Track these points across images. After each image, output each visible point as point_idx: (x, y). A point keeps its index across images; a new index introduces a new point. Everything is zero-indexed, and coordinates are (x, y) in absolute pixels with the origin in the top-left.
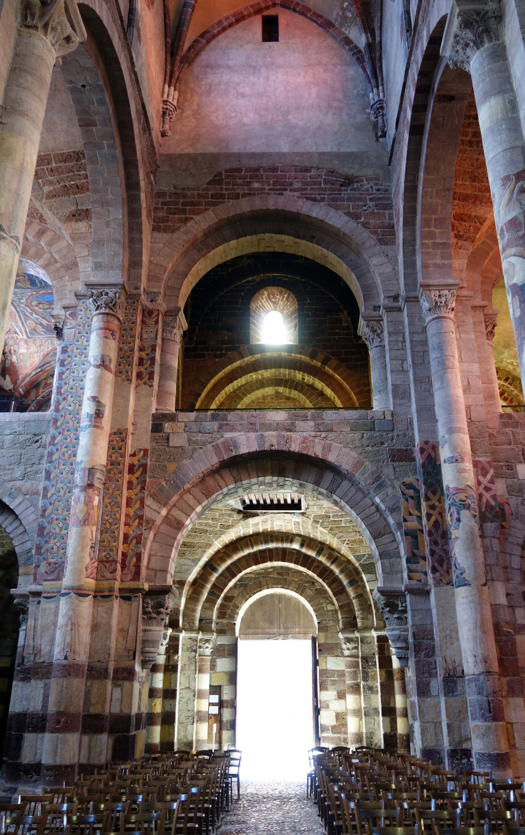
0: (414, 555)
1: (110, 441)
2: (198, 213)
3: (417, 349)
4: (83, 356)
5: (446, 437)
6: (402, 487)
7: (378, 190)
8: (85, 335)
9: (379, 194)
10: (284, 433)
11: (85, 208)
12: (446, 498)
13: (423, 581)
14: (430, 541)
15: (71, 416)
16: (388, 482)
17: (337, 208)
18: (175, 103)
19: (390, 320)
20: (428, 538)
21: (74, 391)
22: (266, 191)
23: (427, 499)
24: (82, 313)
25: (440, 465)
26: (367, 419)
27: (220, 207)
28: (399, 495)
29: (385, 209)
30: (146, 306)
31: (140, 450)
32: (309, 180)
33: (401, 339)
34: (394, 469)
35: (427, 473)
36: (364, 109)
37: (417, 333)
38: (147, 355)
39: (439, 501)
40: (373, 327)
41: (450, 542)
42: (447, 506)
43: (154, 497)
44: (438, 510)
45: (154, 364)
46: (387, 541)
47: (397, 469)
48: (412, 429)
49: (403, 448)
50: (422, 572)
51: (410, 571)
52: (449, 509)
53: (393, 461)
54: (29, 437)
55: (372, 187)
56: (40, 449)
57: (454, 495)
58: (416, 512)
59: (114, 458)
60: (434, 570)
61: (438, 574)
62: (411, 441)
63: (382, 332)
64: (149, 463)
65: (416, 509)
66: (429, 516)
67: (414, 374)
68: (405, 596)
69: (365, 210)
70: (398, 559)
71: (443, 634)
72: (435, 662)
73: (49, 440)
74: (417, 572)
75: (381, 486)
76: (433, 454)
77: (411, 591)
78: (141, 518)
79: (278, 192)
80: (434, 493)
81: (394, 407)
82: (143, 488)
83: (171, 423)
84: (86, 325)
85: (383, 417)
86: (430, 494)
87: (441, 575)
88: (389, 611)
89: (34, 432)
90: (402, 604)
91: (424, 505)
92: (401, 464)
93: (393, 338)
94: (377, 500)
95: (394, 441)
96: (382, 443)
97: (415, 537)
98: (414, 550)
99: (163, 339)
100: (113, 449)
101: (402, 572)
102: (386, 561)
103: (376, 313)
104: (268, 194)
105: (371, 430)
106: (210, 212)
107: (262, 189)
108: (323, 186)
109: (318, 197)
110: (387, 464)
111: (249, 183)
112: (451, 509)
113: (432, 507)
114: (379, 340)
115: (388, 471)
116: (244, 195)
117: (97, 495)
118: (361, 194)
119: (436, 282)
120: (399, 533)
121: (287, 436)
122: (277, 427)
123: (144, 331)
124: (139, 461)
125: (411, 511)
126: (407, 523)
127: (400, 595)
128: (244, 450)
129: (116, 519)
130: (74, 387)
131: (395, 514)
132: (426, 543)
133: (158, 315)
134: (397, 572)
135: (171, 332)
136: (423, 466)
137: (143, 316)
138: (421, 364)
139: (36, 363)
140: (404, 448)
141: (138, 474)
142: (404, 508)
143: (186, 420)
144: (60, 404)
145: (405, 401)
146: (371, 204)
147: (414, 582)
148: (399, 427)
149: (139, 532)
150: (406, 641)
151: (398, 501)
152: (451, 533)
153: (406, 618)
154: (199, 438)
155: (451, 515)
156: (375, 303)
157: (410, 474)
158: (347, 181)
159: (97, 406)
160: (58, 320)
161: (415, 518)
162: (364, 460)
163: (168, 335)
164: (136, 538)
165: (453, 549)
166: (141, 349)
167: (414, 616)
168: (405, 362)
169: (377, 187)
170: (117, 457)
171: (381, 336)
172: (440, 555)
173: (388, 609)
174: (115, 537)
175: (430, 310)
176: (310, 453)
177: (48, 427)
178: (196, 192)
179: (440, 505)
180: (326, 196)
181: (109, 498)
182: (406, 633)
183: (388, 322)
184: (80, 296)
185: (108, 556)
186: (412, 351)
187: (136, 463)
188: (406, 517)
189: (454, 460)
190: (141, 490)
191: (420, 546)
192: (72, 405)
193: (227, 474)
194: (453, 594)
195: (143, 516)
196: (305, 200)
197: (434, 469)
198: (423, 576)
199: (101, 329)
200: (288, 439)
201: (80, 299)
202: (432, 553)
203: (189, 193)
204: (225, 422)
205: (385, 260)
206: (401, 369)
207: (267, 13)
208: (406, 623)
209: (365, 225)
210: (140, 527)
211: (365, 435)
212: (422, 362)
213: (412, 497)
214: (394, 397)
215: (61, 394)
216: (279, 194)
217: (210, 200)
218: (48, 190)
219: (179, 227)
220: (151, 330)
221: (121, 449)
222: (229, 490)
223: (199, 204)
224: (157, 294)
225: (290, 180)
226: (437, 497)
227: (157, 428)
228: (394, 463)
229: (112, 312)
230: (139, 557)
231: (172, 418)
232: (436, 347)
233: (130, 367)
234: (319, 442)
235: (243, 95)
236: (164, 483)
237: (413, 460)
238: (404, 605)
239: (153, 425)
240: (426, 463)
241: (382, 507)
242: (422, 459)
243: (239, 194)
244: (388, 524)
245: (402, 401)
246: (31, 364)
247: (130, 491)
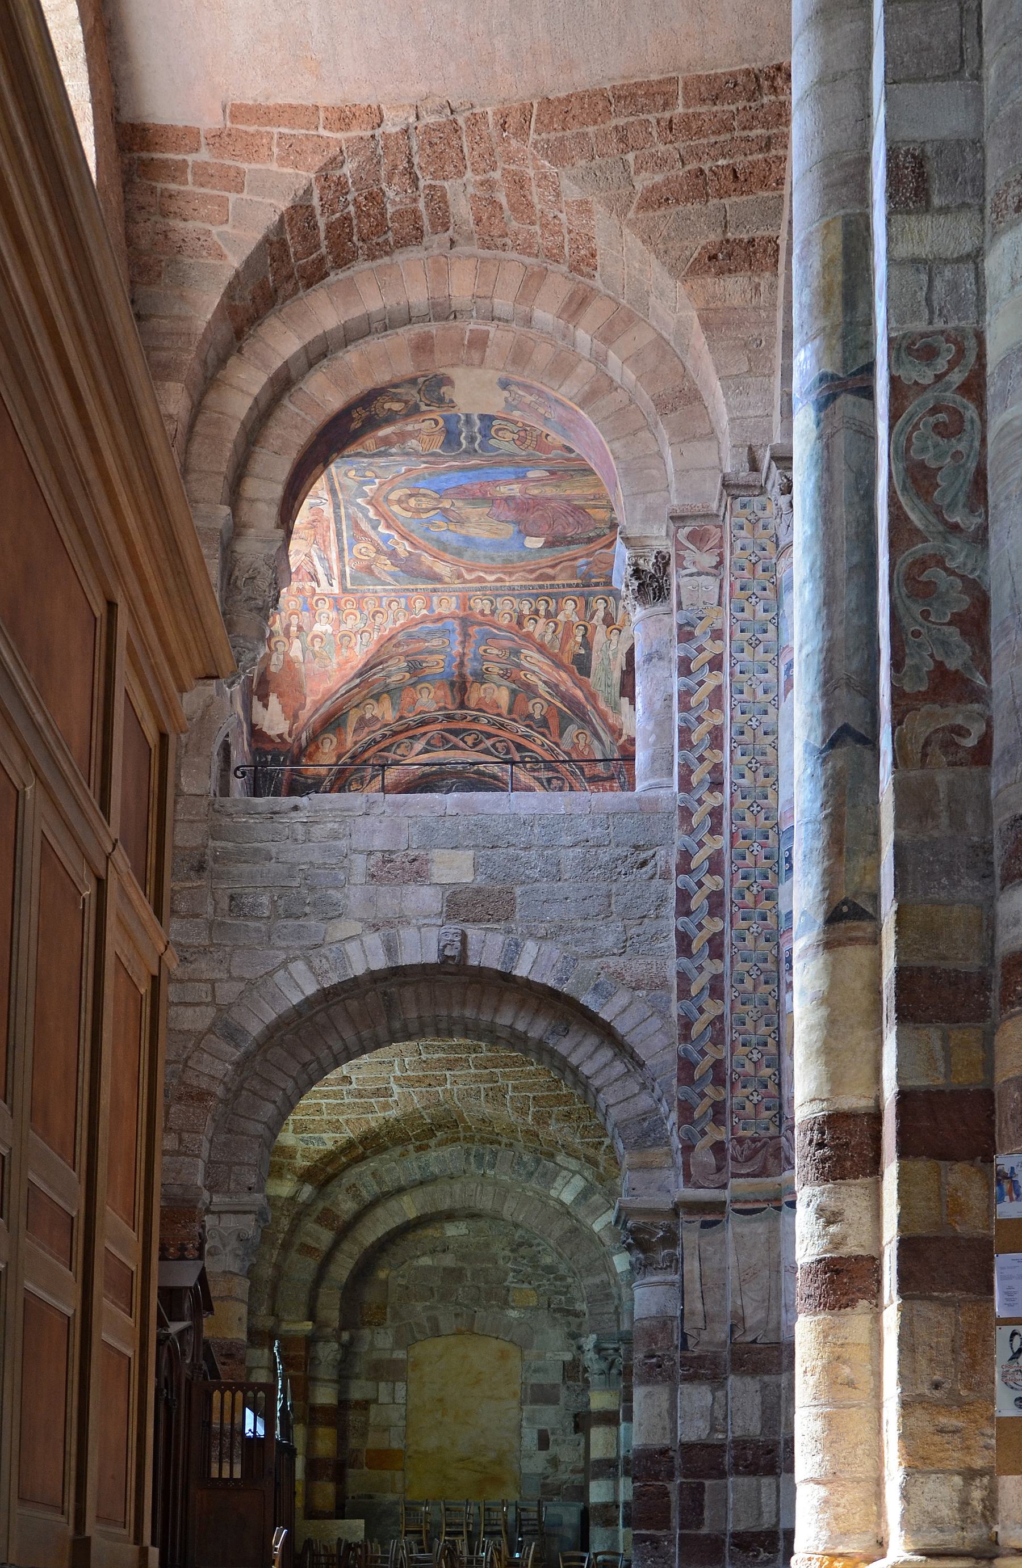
8: (759, 593)
15: (748, 802)
21: (747, 738)
54: (623, 851)
56: (657, 882)
73: (674, 860)
89: (633, 841)
130: (747, 729)
139: (354, 663)
144: (692, 772)
177: (669, 829)
184: (737, 486)
192: (748, 773)
215: (693, 747)
246: (341, 666)
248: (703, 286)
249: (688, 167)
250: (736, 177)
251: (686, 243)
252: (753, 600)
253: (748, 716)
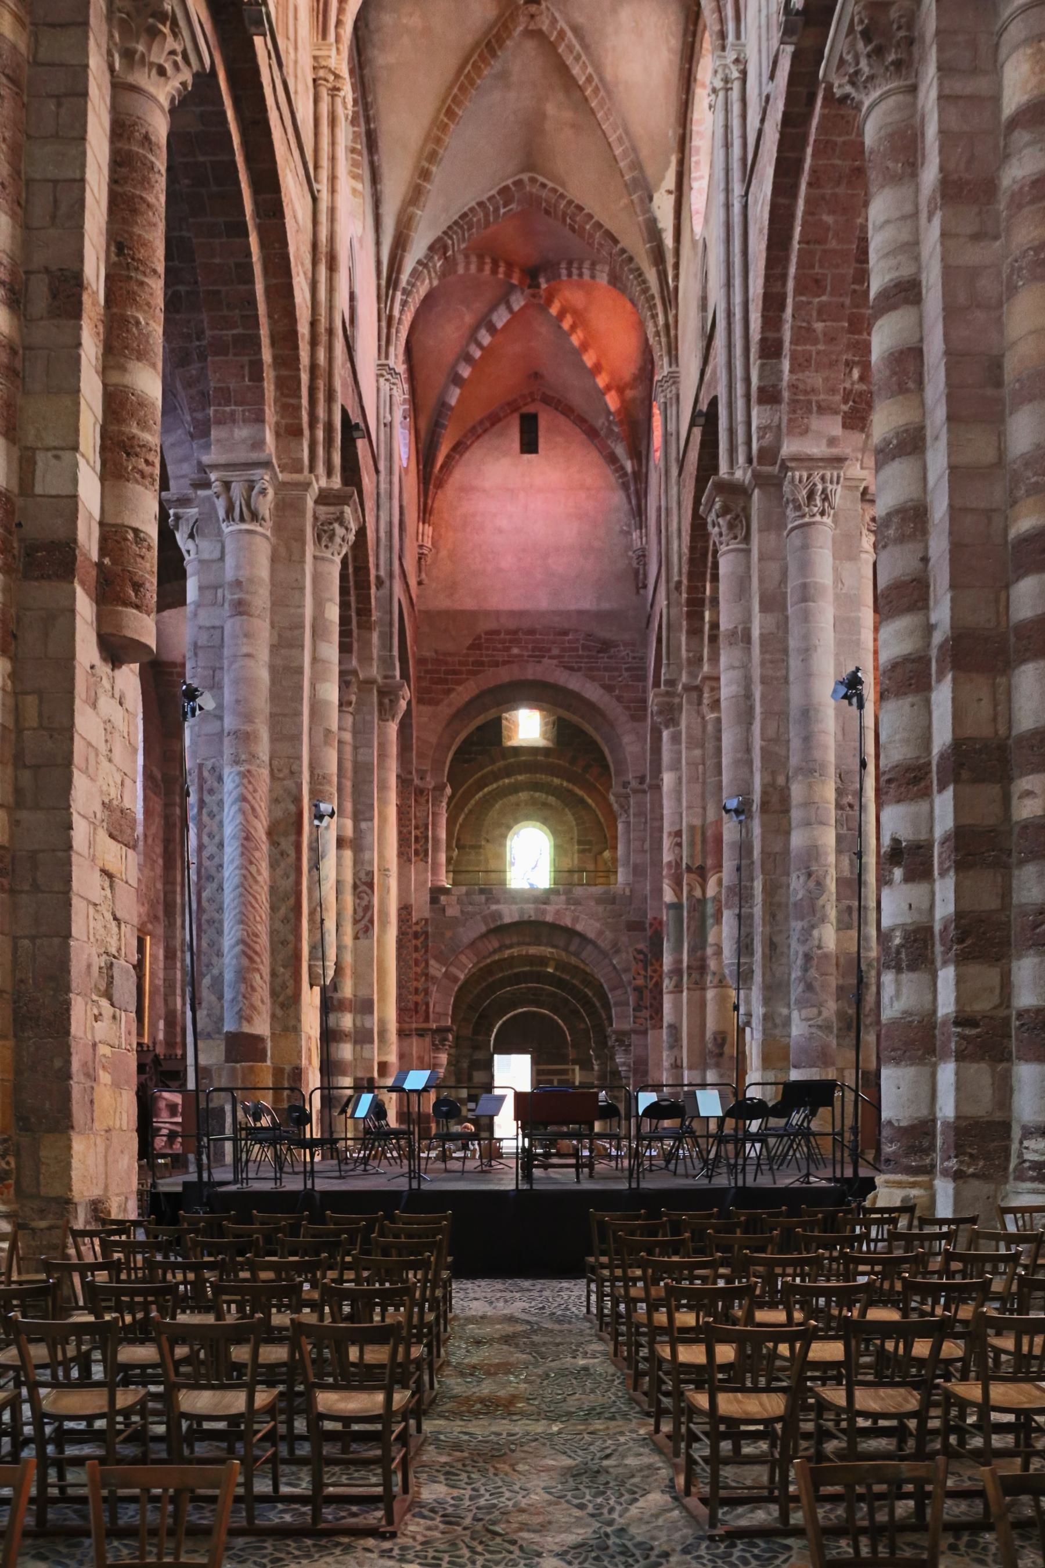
2: (459, 683)
17: (593, 679)
18: (429, 545)
36: (626, 552)
43: (436, 958)
51: (635, 1017)
78: (427, 975)
82: (426, 951)
111: (508, 649)
113: (655, 971)
115: (624, 939)
116: (505, 663)
128: (507, 920)
141: (422, 939)
146: (626, 674)
163: (437, 810)
166: (416, 828)
178: (456, 659)
202: (651, 1005)
203: (449, 659)
207: (525, 410)
209: (619, 699)
223: (460, 672)
224: (426, 771)
227: (434, 900)
230: (427, 1005)
235: (500, 531)
237: (645, 930)
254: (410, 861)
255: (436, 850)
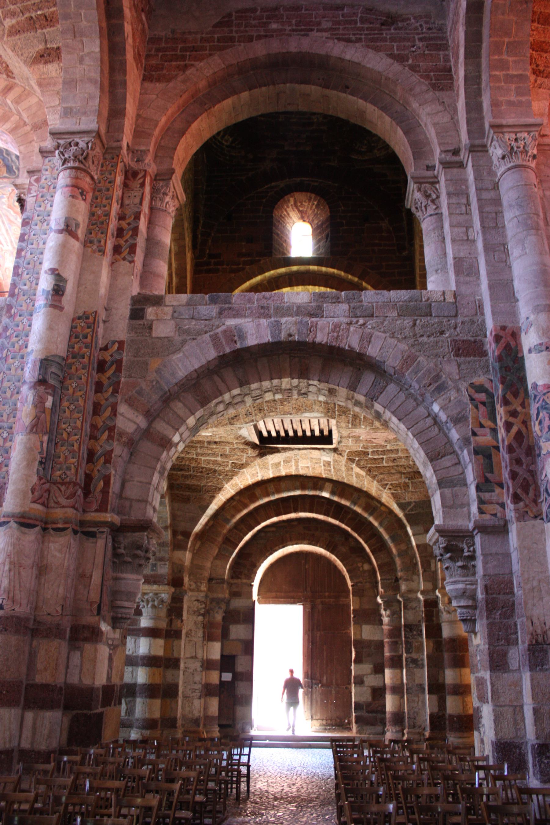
0: (487, 480)
1: (73, 328)
2: (200, 59)
3: (487, 209)
4: (45, 223)
5: (532, 317)
6: (470, 390)
7: (429, 29)
8: (49, 198)
9: (432, 33)
10: (306, 319)
11: (55, 46)
12: (532, 401)
13: (499, 515)
14: (511, 459)
15: (25, 298)
16: (450, 383)
17: (377, 49)
19: (449, 178)
20: (507, 456)
21: (30, 266)
22: (287, 32)
23: (506, 402)
24: (47, 173)
25: (523, 357)
26: (421, 301)
27: (228, 51)
28: (465, 401)
29: (439, 50)
30: (129, 166)
31: (114, 342)
32: (341, 18)
33: (464, 201)
34: (459, 366)
35: (506, 368)
37: (487, 189)
38: (129, 224)
39: (523, 405)
40: (425, 192)
41: (539, 460)
42: (533, 412)
44: (520, 417)
45: (137, 235)
46: (449, 464)
47: (463, 366)
48: (482, 314)
49: (470, 338)
50: (498, 504)
51: (481, 502)
52: (538, 414)
53: (457, 355)
55: (421, 26)
57: (544, 394)
58: (490, 423)
59: (76, 349)
60: (516, 498)
61: (521, 504)
62: (481, 330)
63: (438, 197)
64: (125, 358)
65: (490, 419)
66: (508, 426)
67: (485, 240)
68: (472, 537)
69: (413, 52)
70: (464, 489)
71: (529, 586)
72: (516, 625)
74: (492, 503)
75: (441, 389)
76: (512, 343)
77: (482, 528)
78: (111, 429)
79: (303, 33)
80: (516, 395)
81: (457, 286)
83: (155, 308)
84: (52, 187)
85: (442, 298)
86: (509, 396)
87: (526, 506)
88: (451, 558)
90: (469, 547)
91: (501, 411)
92: (468, 359)
93: (454, 200)
94: (436, 408)
95: (458, 329)
96: (442, 333)
97: (489, 457)
98: (487, 474)
99: (151, 209)
100: (77, 337)
101: (469, 505)
102: (447, 491)
103: (429, 173)
104: (290, 35)
105: (427, 315)
106: (216, 57)
107: (281, 30)
108: (359, 25)
109: (354, 38)
110: (449, 361)
112: (541, 415)
113: (514, 414)
114: (434, 207)
116: (259, 37)
117: (50, 395)
118: (407, 34)
119: (511, 121)
120: (465, 452)
121: (312, 322)
122: (300, 310)
123: (125, 195)
124: (112, 356)
125: (483, 421)
126: (477, 438)
127: (467, 536)
128: (251, 341)
129: (76, 428)
130: (32, 262)
131: (461, 425)
132: (503, 464)
133: (144, 176)
134: (462, 506)
135: (162, 200)
136: (500, 359)
137: (126, 178)
138: (493, 228)
140: (472, 339)
142: (473, 418)
143: (175, 303)
145: (471, 279)
147: (487, 517)
148: (465, 312)
149: (108, 448)
150: (473, 597)
151: (465, 409)
152: (540, 448)
153: (474, 566)
154: (191, 326)
155: (540, 423)
156: (427, 162)
157: (480, 373)
158: (390, 20)
159: (56, 280)
160: (22, 191)
161: (488, 430)
162: (418, 354)
164: (105, 455)
165: (543, 468)
166: (121, 217)
167: (487, 563)
168: (471, 229)
169: (428, 26)
170: (80, 348)
171: (436, 202)
172: (525, 479)
173: (448, 555)
174: (74, 451)
175: (503, 158)
176: (342, 345)
179: (524, 410)
180: (363, 37)
181: (68, 400)
182: (474, 587)
183: (446, 180)
184: (46, 152)
185: (64, 476)
186: (481, 212)
187: (108, 358)
188: (476, 430)
189: (544, 348)
190: (113, 393)
191: (495, 469)
192: (28, 283)
193: (229, 374)
194: (543, 531)
195: (114, 426)
196: (336, 41)
197: (514, 362)
198: (499, 509)
199: (67, 186)
200: (312, 327)
201: (46, 157)
202: (514, 475)
203: (190, 37)
204: (227, 306)
205: (440, 108)
206: (465, 238)
208: (474, 574)
209: (413, 68)
210: (111, 441)
211: (418, 322)
212: (494, 225)
213: (484, 404)
214: (458, 272)
216: (303, 35)
217: (216, 44)
218: (10, 24)
219: (176, 75)
220: (135, 194)
221: (86, 338)
222: (233, 397)
223: (203, 49)
225: (318, 20)
226: (520, 400)
228: (458, 359)
229: (82, 166)
230: (107, 480)
231: (158, 301)
232: (514, 203)
233: (103, 235)
234: (355, 331)
236: (143, 385)
237: (484, 354)
238: (471, 549)
239: (132, 310)
240: (503, 355)
241: (443, 417)
242: (498, 350)
243: (252, 36)
244: (449, 442)
245: (468, 279)
247: (99, 394)
248: (39, 69)
249: (26, 16)
250: (47, 20)
251: (30, 50)
252: (46, 202)
253: (33, 255)
254: (102, 252)
255: (149, 254)
